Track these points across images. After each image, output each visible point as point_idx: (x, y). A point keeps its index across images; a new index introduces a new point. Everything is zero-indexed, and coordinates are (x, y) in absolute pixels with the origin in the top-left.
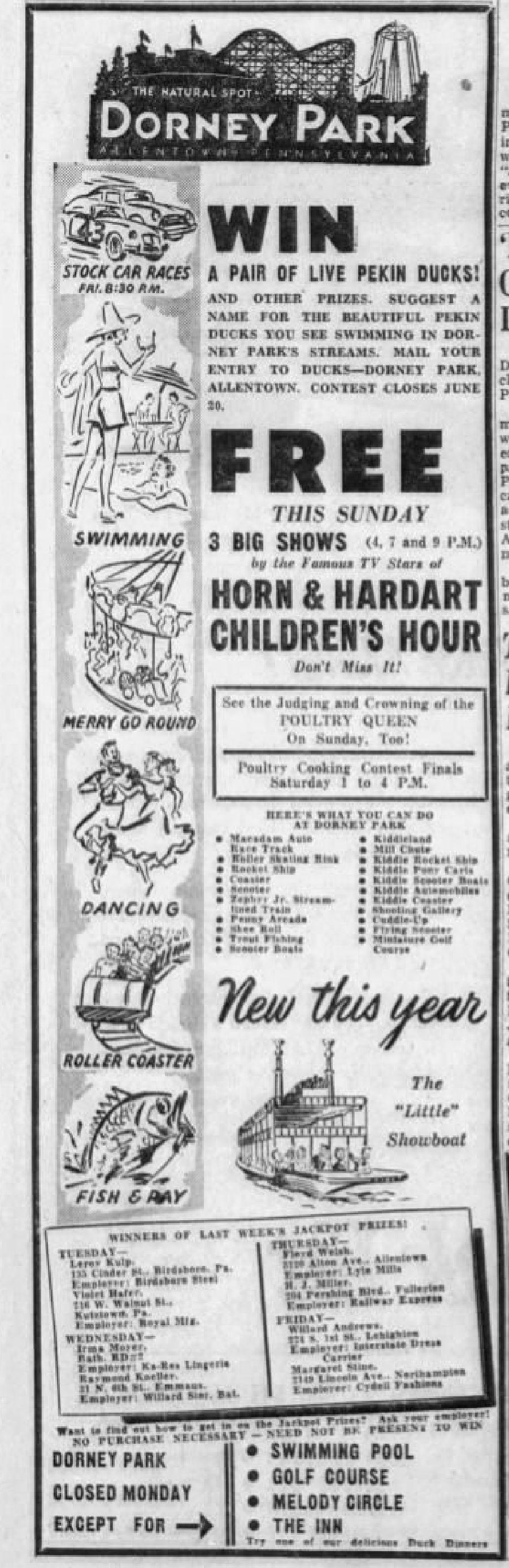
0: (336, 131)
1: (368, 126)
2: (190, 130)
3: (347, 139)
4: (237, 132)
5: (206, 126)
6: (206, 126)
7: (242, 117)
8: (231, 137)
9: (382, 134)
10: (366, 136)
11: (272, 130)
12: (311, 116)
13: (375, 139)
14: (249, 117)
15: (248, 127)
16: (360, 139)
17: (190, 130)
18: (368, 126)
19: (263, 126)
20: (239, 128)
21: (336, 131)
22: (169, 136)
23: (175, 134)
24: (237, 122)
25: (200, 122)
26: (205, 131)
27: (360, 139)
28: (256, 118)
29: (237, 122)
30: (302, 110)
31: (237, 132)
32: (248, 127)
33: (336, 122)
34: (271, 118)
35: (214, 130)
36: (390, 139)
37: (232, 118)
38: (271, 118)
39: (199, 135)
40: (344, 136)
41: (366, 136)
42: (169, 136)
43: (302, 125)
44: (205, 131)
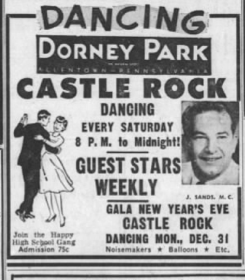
0: (166, 54)
1: (183, 51)
2: (88, 54)
3: (172, 58)
4: (112, 55)
5: (96, 52)
6: (96, 52)
7: (115, 46)
8: (109, 57)
9: (191, 55)
10: (182, 56)
11: (130, 54)
12: (152, 46)
13: (187, 58)
14: (118, 46)
15: (119, 52)
16: (179, 58)
17: (88, 54)
18: (183, 51)
19: (127, 52)
20: (113, 52)
21: (166, 54)
22: (76, 57)
23: (79, 56)
24: (112, 49)
25: (93, 50)
26: (95, 55)
27: (179, 58)
28: (122, 47)
29: (112, 49)
30: (147, 42)
31: (112, 55)
32: (119, 52)
33: (166, 49)
34: (131, 47)
35: (100, 53)
36: (195, 58)
37: (109, 46)
38: (131, 47)
39: (92, 57)
40: (170, 56)
41: (182, 56)
42: (76, 57)
43: (148, 51)
44: (95, 54)
